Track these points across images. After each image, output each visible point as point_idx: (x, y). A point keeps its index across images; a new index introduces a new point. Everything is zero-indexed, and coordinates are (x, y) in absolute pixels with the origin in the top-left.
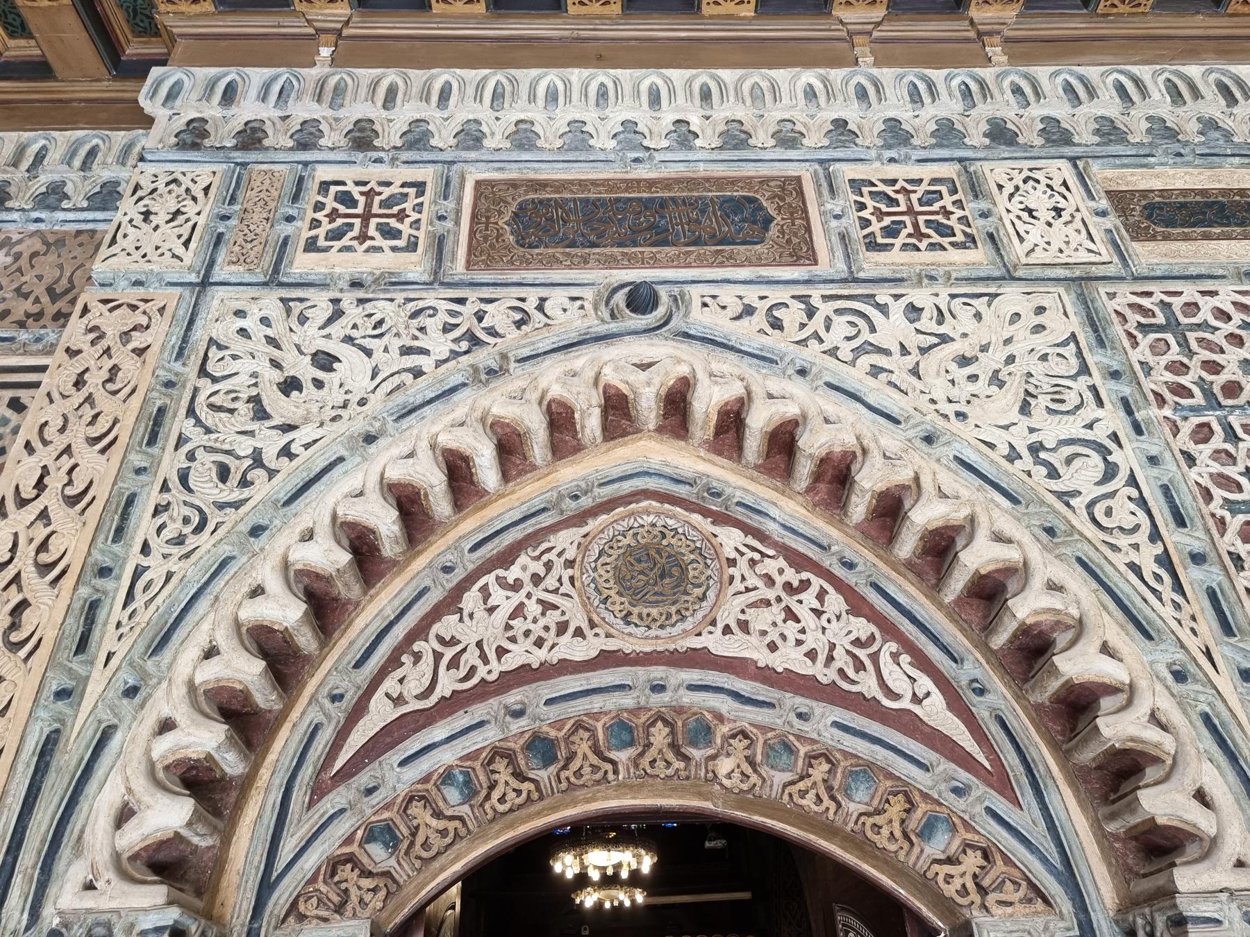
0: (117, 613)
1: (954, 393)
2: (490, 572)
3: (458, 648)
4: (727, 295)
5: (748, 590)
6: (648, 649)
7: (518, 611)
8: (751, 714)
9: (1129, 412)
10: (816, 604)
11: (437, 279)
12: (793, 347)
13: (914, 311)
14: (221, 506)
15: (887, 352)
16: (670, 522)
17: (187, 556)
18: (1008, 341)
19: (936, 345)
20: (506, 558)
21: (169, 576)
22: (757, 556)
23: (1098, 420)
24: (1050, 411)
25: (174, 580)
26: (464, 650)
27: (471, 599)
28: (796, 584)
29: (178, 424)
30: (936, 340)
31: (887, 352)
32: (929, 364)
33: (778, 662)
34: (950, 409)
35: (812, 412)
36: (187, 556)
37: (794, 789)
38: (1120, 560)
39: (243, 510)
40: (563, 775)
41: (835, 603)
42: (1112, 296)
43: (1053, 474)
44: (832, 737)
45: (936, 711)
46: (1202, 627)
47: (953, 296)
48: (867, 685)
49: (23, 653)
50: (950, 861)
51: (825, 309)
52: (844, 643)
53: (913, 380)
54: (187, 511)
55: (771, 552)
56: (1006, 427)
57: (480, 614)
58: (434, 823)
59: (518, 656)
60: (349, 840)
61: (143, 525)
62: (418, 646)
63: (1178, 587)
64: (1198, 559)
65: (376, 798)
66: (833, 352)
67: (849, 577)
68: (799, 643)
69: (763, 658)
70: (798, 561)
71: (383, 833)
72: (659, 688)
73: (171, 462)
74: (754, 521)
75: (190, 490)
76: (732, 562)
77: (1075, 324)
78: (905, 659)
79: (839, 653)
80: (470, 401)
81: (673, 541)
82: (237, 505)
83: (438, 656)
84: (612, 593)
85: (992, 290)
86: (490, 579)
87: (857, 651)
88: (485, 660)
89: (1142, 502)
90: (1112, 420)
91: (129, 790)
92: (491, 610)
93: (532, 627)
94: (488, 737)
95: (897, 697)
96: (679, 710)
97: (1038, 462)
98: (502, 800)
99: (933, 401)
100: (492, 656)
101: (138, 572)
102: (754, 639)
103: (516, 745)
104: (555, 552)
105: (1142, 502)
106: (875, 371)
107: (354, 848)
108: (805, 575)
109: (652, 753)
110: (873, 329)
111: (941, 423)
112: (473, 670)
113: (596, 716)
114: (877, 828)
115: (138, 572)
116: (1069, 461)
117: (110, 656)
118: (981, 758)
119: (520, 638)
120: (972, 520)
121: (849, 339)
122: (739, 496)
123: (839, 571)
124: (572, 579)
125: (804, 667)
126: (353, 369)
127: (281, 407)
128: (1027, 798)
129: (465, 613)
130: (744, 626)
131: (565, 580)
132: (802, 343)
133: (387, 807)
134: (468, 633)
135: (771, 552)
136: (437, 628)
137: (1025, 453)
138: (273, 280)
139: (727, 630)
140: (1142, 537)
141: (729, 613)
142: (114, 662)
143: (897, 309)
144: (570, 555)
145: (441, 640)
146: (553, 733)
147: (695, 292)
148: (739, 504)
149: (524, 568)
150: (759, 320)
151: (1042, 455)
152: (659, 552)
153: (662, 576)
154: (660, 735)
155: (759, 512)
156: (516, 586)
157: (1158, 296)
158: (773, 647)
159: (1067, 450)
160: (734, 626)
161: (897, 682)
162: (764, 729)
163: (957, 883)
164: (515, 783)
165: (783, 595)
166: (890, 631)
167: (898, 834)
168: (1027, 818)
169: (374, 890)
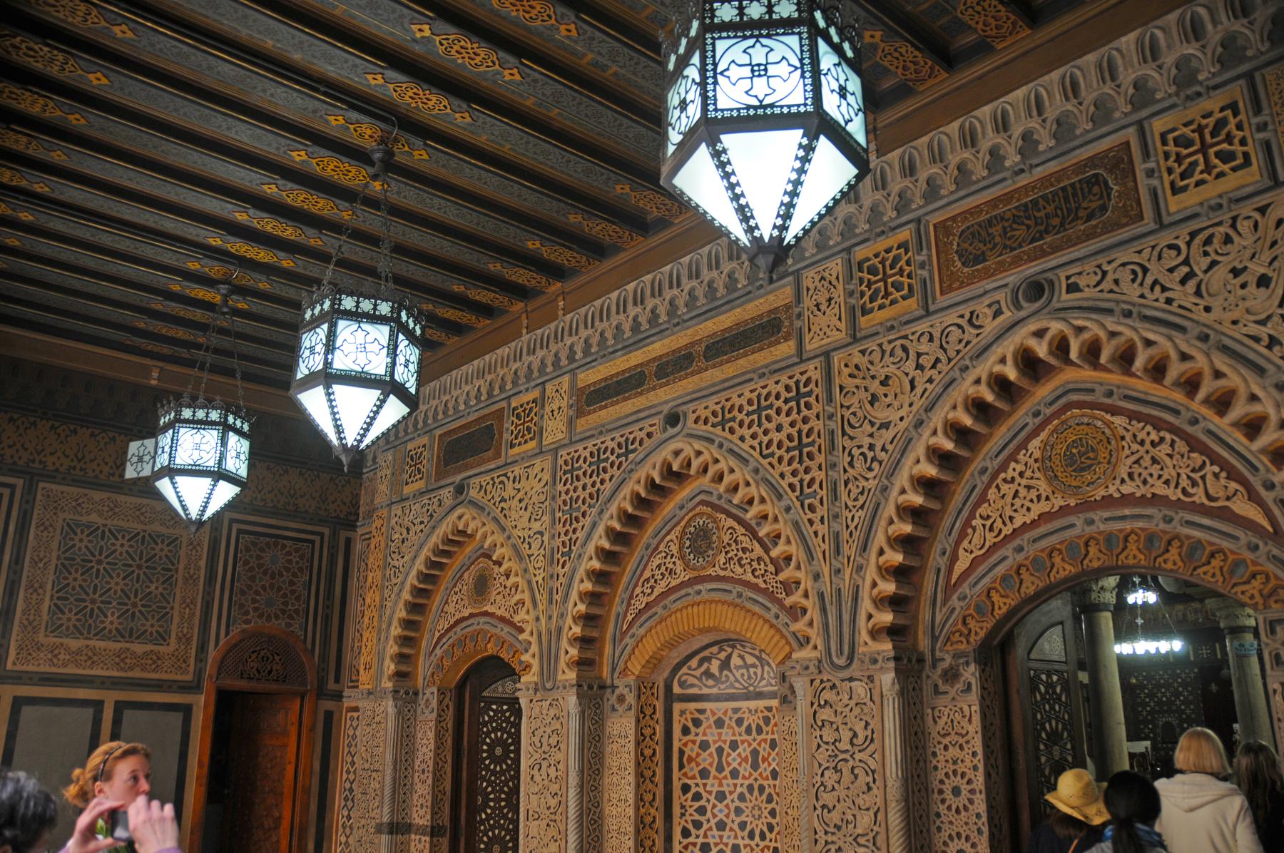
4: (476, 480)
20: (455, 586)
29: (389, 559)
33: (499, 613)
51: (497, 481)
106: (503, 509)
147: (472, 481)
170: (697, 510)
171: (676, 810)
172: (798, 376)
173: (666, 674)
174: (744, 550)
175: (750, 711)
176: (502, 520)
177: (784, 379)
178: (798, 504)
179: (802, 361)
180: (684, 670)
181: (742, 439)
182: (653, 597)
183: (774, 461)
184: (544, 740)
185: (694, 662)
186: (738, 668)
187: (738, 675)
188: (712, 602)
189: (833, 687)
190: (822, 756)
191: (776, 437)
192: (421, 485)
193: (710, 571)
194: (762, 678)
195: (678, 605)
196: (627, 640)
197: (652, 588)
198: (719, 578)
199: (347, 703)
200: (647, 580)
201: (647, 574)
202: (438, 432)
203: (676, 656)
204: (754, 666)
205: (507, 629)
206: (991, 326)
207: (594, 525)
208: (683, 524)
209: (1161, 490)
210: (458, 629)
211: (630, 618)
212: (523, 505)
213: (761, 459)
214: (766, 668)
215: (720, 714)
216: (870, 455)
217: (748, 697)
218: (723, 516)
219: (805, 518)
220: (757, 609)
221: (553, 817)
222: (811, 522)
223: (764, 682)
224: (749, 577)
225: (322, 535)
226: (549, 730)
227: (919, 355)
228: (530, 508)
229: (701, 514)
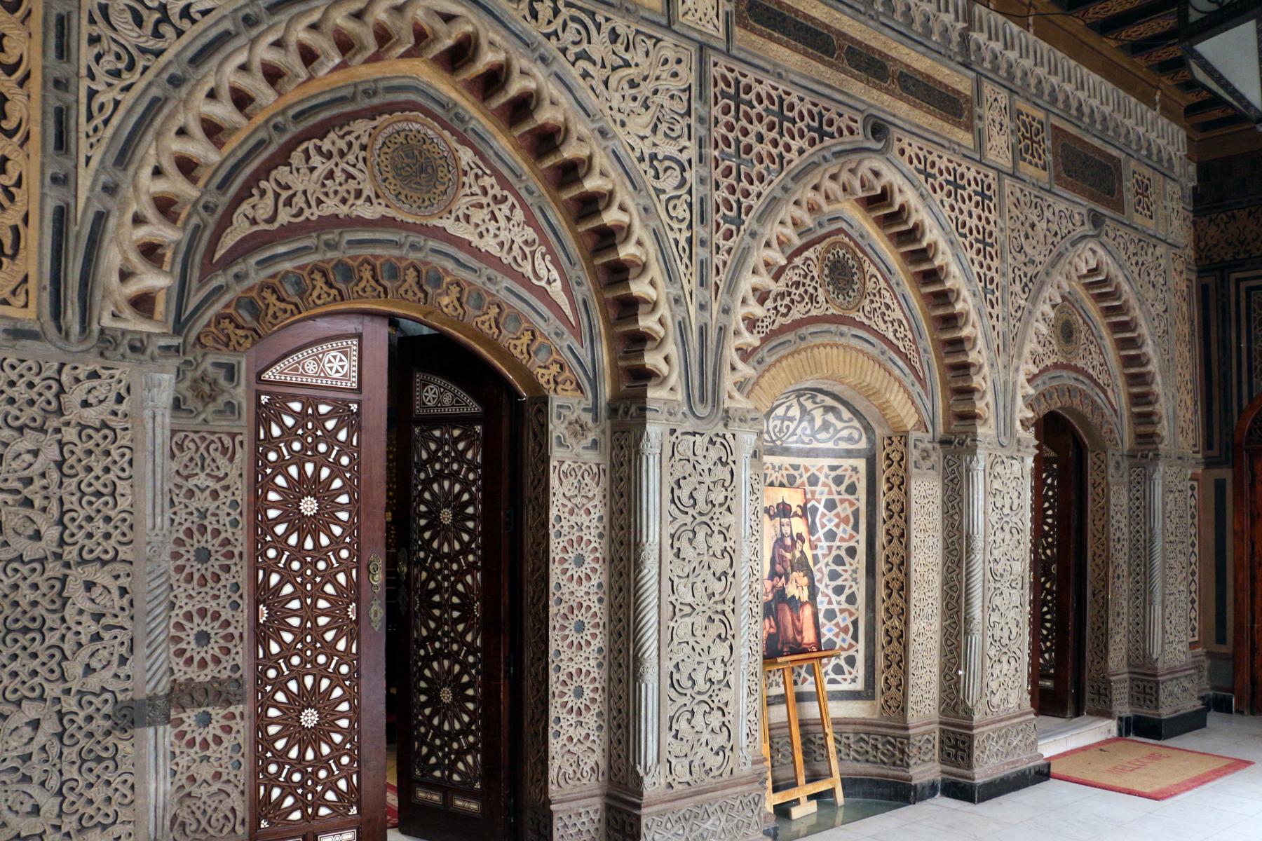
0: (84, 127)
1: (623, 106)
2: (310, 139)
3: (290, 192)
5: (472, 194)
6: (410, 221)
7: (330, 175)
8: (464, 275)
9: (700, 147)
10: (508, 214)
12: (541, 38)
13: (614, 36)
14: (144, 51)
15: (594, 63)
16: (430, 132)
17: (127, 89)
18: (658, 78)
19: (620, 67)
20: (321, 131)
21: (117, 103)
22: (480, 173)
23: (685, 148)
24: (666, 135)
25: (122, 110)
26: (294, 195)
27: (297, 157)
28: (499, 197)
30: (621, 63)
31: (594, 63)
32: (613, 83)
34: (618, 117)
35: (545, 95)
36: (127, 89)
37: (479, 320)
38: (671, 235)
39: (164, 59)
40: (355, 289)
41: (519, 215)
42: (716, 64)
43: (657, 177)
44: (504, 295)
45: (556, 290)
46: (693, 281)
47: (638, 32)
48: (527, 269)
49: (17, 139)
50: (545, 367)
52: (519, 241)
53: (603, 87)
54: (115, 48)
55: (488, 172)
56: (643, 138)
57: (304, 170)
58: (278, 303)
59: (331, 207)
60: (227, 306)
62: (263, 184)
63: (690, 258)
64: (703, 243)
65: (246, 284)
66: (564, 51)
67: (529, 200)
68: (496, 236)
69: (476, 241)
70: (503, 183)
72: (413, 247)
74: (481, 146)
75: (115, 29)
76: (465, 173)
77: (692, 79)
78: (548, 257)
79: (515, 247)
80: (323, 9)
81: (430, 147)
82: (158, 53)
83: (277, 196)
84: (389, 176)
85: (659, 36)
86: (310, 145)
87: (525, 248)
88: (310, 206)
89: (690, 205)
90: (692, 152)
91: (127, 259)
92: (312, 169)
93: (339, 188)
95: (539, 279)
96: (425, 263)
97: (652, 166)
98: (319, 297)
99: (611, 108)
100: (313, 203)
101: (92, 94)
102: (471, 228)
103: (329, 267)
104: (354, 135)
105: (690, 205)
106: (585, 75)
107: (231, 311)
108: (506, 193)
109: (406, 286)
110: (589, 42)
111: (612, 124)
112: (301, 211)
113: (376, 257)
114: (515, 346)
115: (92, 94)
116: (666, 170)
117: (88, 159)
118: (572, 320)
119: (332, 195)
120: (611, 193)
121: (575, 43)
122: (473, 124)
123: (523, 193)
124: (365, 160)
125: (495, 251)
128: (587, 343)
129: (294, 167)
130: (467, 218)
131: (360, 159)
132: (548, 36)
133: (250, 289)
134: (299, 182)
135: (488, 172)
136: (274, 173)
137: (647, 159)
139: (457, 219)
140: (684, 226)
142: (94, 164)
144: (365, 140)
145: (278, 183)
146: (350, 262)
148: (473, 130)
149: (333, 143)
151: (655, 163)
152: (420, 153)
153: (421, 171)
154: (411, 274)
155: (483, 139)
156: (329, 156)
157: (736, 74)
158: (481, 235)
159: (667, 163)
160: (461, 216)
161: (543, 272)
162: (470, 284)
163: (546, 378)
164: (325, 288)
165: (492, 203)
166: (544, 240)
167: (525, 351)
168: (585, 354)
169: (246, 337)
174: (888, 307)
175: (774, 467)
182: (787, 320)
184: (700, 496)
188: (852, 348)
190: (994, 518)
193: (853, 314)
194: (794, 433)
195: (818, 341)
198: (862, 325)
204: (791, 419)
206: (1080, 231)
207: (774, 202)
208: (824, 244)
209: (1090, 371)
216: (1024, 280)
218: (868, 261)
220: (897, 372)
221: (720, 607)
223: (794, 438)
224: (891, 336)
226: (707, 480)
227: (1048, 221)
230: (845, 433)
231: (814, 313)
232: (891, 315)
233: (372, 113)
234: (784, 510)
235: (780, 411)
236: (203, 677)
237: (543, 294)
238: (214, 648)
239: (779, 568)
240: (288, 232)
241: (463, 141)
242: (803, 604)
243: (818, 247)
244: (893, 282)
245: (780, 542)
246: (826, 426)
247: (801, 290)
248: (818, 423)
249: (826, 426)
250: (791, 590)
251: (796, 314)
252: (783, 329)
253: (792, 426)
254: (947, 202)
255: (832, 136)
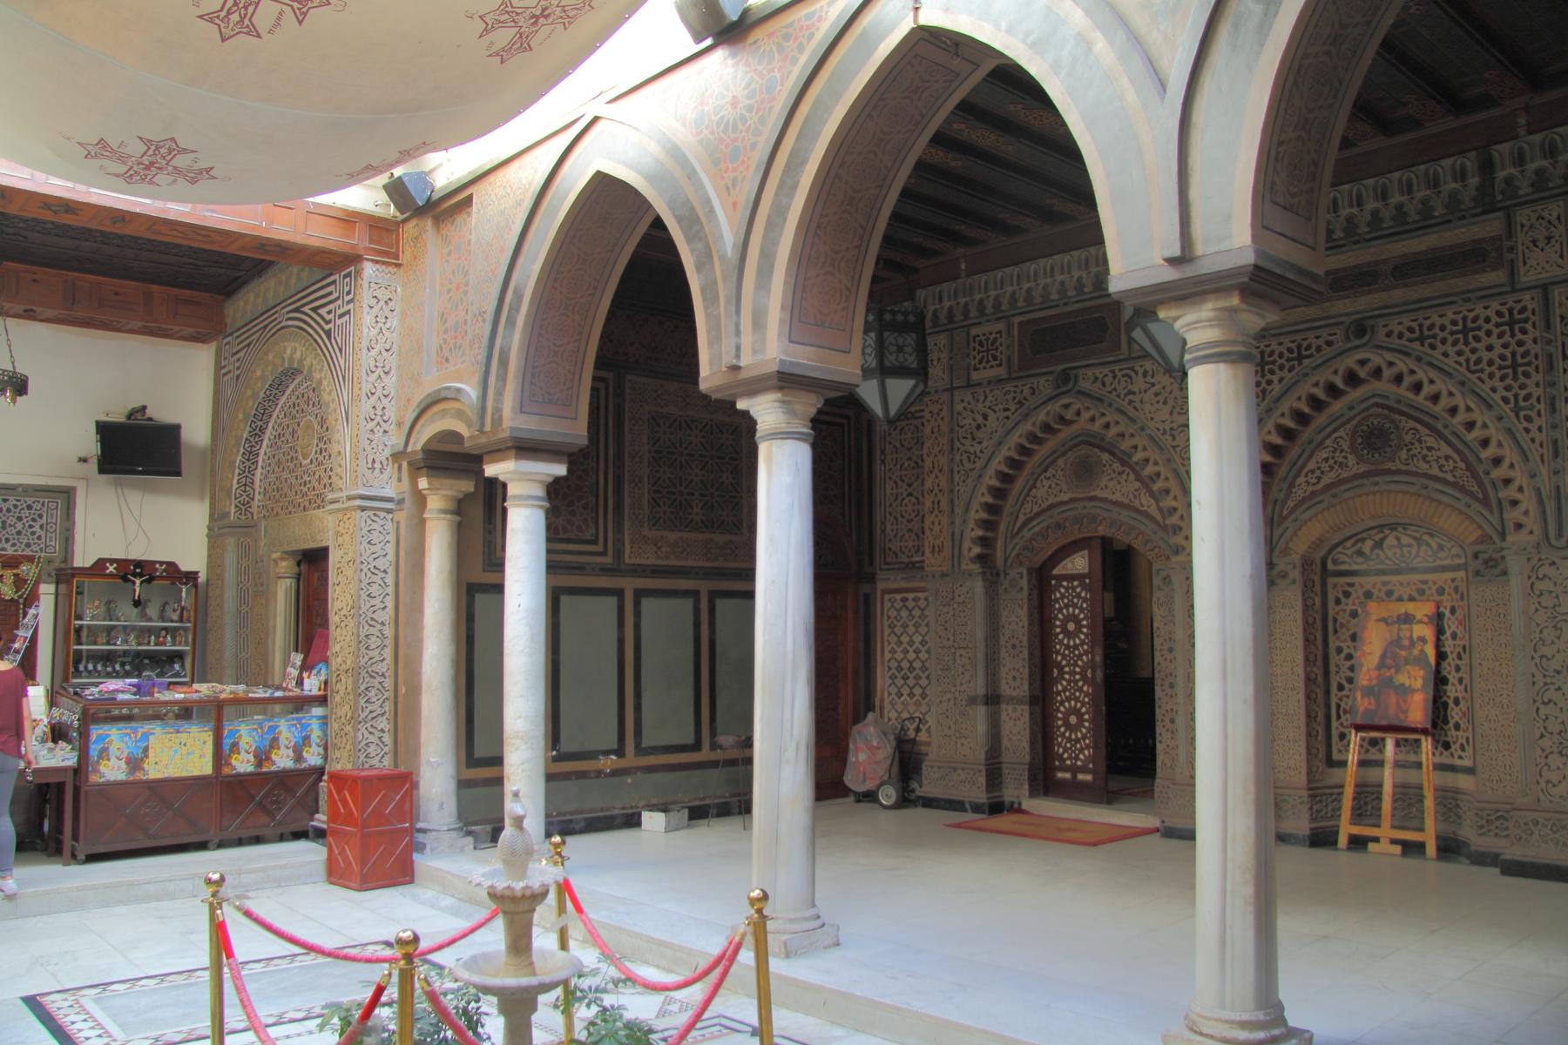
11: (1010, 379)
20: (1045, 471)
29: (957, 444)
33: (1114, 498)
41: (1132, 477)
48: (1136, 503)
51: (1119, 374)
61: (956, 477)
70: (1123, 463)
71: (1026, 548)
73: (957, 459)
94: (1045, 524)
106: (1131, 402)
126: (992, 417)
127: (979, 434)
138: (969, 386)
141: (1103, 483)
143: (1141, 371)
147: (1081, 372)
150: (1099, 384)
161: (1144, 502)
170: (1371, 411)
171: (1333, 669)
172: (1511, 304)
173: (1323, 553)
174: (1430, 449)
176: (1132, 413)
177: (1495, 305)
178: (1512, 415)
179: (1514, 291)
180: (1340, 549)
181: (1446, 355)
182: (1319, 487)
183: (1485, 376)
185: (1349, 544)
186: (1390, 547)
187: (1390, 554)
189: (1553, 563)
191: (1486, 356)
192: (1001, 372)
195: (1350, 494)
196: (1288, 523)
197: (1319, 478)
198: (1398, 472)
199: (880, 586)
200: (1313, 471)
201: (1311, 465)
202: (1017, 320)
203: (1338, 537)
204: (1409, 546)
205: (1125, 513)
208: (1354, 422)
210: (1055, 512)
211: (1291, 504)
212: (1160, 398)
213: (1469, 375)
214: (1424, 547)
215: (1368, 587)
217: (1398, 572)
219: (1521, 427)
220: (1445, 499)
222: (1527, 430)
224: (1435, 471)
225: (847, 417)
228: (1171, 403)
229: (1378, 415)
230: (1454, 551)
231: (1344, 475)
232: (1432, 456)
233: (1064, 454)
234: (1407, 619)
235: (1390, 541)
236: (1015, 694)
237: (1146, 514)
238: (1018, 682)
239: (1389, 662)
240: (1038, 515)
241: (1102, 449)
242: (1413, 691)
243: (1349, 426)
244: (1439, 426)
245: (1396, 642)
246: (1441, 548)
247: (1331, 462)
248: (1435, 546)
249: (1441, 548)
250: (1401, 679)
251: (1325, 481)
252: (1313, 494)
253: (1414, 551)
254: (1451, 351)
255: (1311, 356)
